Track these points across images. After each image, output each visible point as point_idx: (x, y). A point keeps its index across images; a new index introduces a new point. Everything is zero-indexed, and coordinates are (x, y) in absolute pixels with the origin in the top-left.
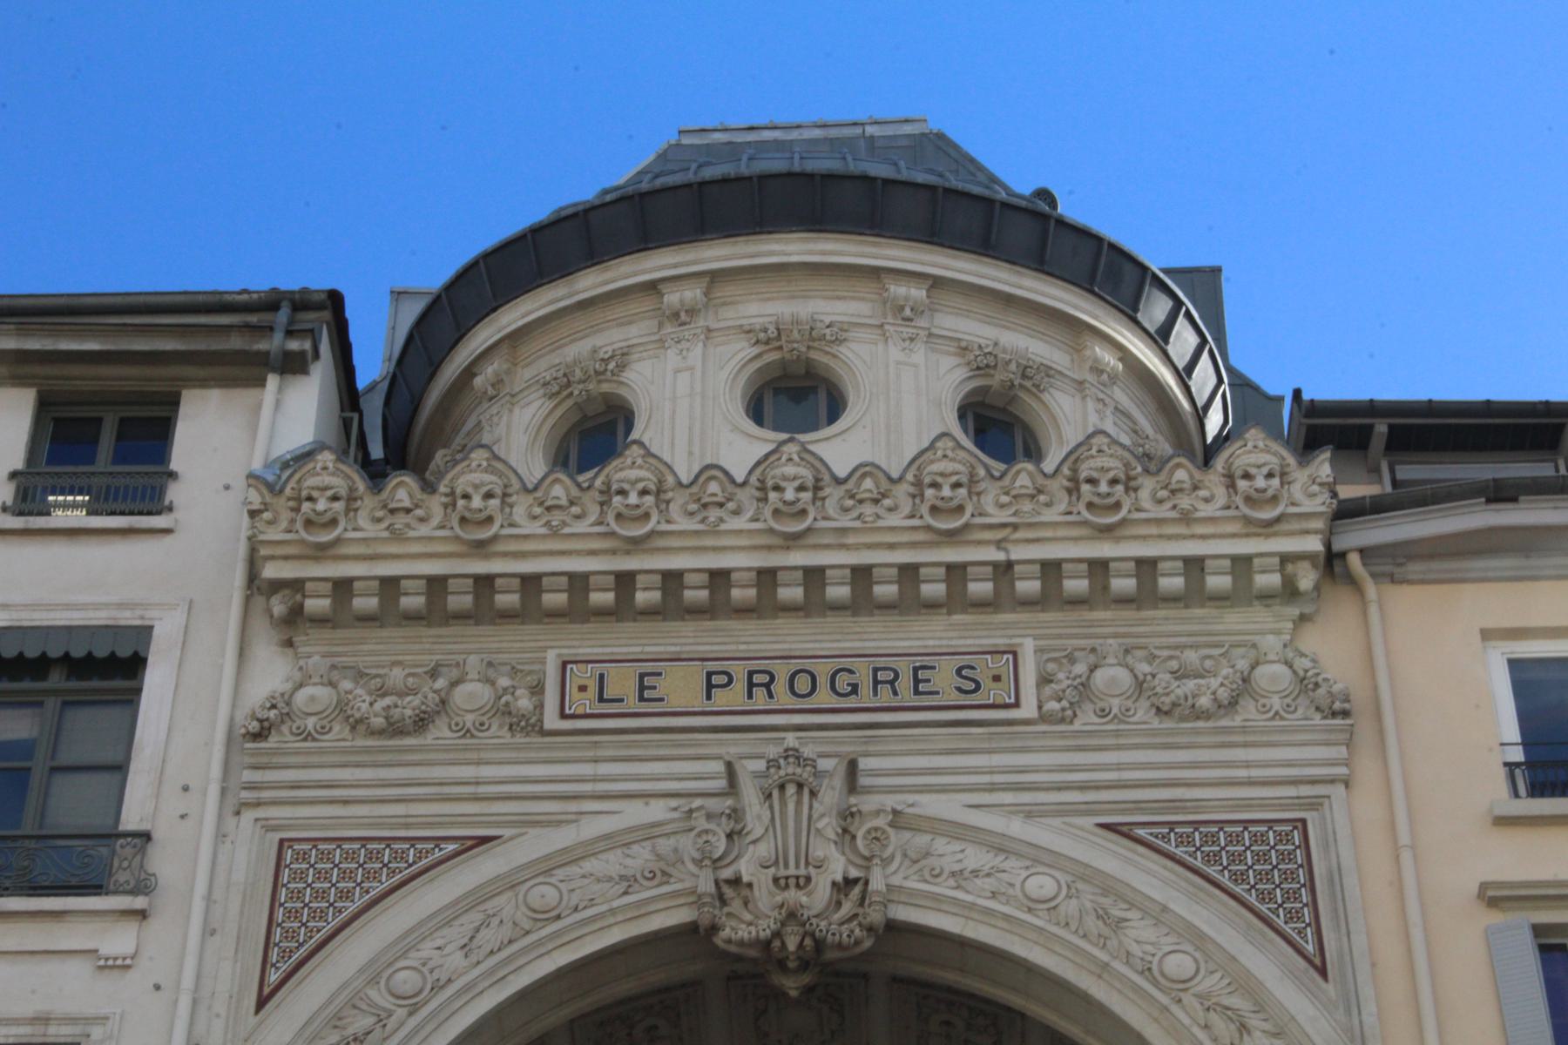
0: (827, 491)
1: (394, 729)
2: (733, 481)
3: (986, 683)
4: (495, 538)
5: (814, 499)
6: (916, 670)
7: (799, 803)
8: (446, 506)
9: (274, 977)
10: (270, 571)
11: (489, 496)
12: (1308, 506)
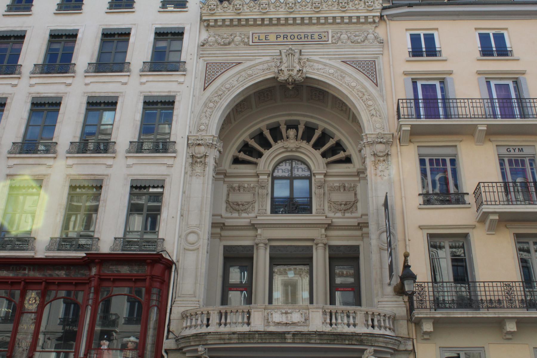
0: (297, 4)
1: (225, 44)
2: (281, 2)
3: (323, 37)
4: (241, 12)
5: (295, 6)
6: (311, 35)
7: (292, 57)
8: (233, 7)
9: (206, 85)
10: (204, 18)
11: (240, 5)
12: (378, 7)
